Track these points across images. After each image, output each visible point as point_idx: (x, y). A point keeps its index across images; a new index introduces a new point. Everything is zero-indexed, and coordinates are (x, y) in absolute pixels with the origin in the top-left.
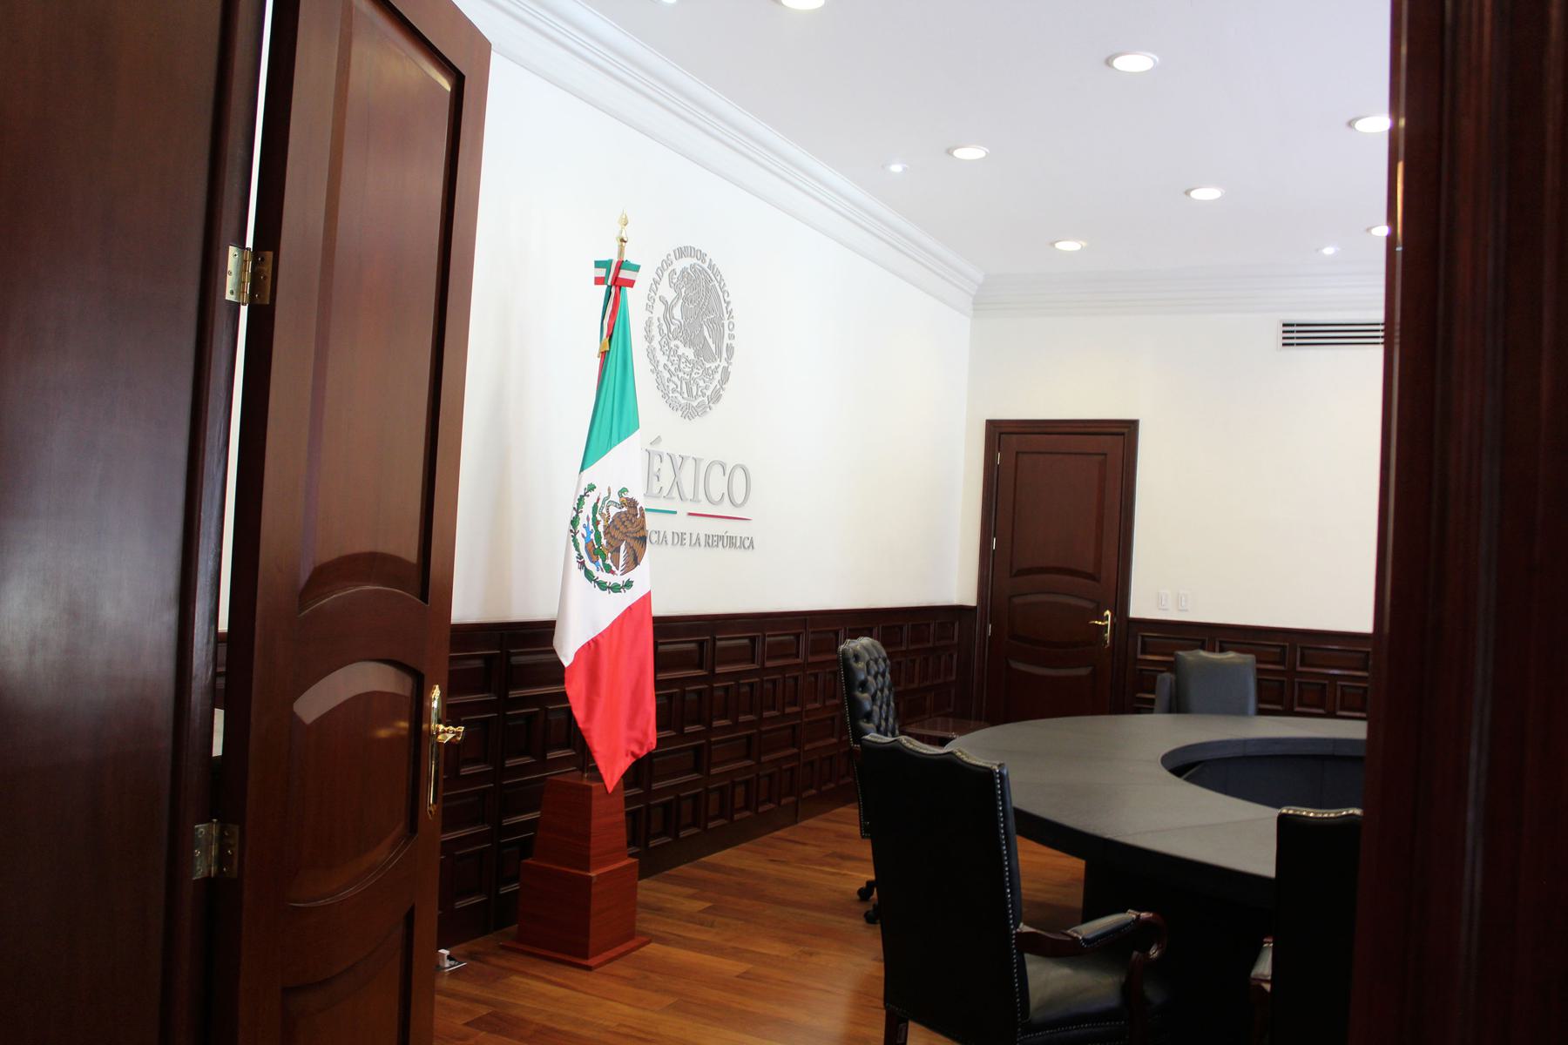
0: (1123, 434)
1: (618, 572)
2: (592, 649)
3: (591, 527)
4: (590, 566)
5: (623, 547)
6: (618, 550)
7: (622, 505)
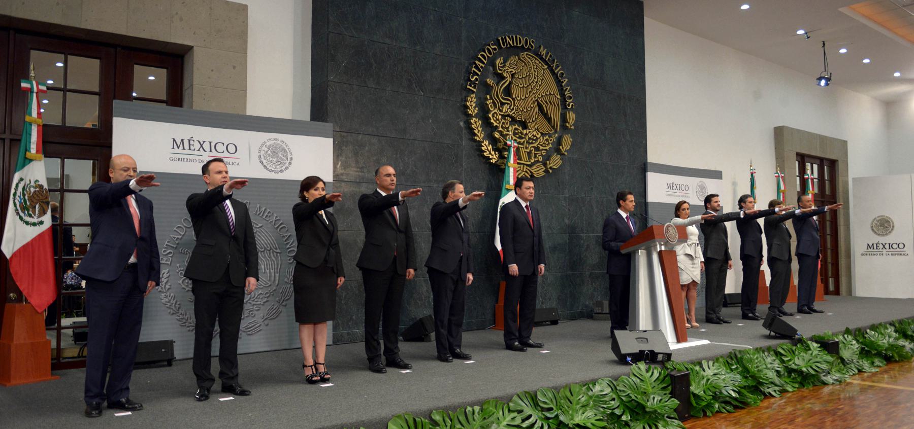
0: (722, 179)
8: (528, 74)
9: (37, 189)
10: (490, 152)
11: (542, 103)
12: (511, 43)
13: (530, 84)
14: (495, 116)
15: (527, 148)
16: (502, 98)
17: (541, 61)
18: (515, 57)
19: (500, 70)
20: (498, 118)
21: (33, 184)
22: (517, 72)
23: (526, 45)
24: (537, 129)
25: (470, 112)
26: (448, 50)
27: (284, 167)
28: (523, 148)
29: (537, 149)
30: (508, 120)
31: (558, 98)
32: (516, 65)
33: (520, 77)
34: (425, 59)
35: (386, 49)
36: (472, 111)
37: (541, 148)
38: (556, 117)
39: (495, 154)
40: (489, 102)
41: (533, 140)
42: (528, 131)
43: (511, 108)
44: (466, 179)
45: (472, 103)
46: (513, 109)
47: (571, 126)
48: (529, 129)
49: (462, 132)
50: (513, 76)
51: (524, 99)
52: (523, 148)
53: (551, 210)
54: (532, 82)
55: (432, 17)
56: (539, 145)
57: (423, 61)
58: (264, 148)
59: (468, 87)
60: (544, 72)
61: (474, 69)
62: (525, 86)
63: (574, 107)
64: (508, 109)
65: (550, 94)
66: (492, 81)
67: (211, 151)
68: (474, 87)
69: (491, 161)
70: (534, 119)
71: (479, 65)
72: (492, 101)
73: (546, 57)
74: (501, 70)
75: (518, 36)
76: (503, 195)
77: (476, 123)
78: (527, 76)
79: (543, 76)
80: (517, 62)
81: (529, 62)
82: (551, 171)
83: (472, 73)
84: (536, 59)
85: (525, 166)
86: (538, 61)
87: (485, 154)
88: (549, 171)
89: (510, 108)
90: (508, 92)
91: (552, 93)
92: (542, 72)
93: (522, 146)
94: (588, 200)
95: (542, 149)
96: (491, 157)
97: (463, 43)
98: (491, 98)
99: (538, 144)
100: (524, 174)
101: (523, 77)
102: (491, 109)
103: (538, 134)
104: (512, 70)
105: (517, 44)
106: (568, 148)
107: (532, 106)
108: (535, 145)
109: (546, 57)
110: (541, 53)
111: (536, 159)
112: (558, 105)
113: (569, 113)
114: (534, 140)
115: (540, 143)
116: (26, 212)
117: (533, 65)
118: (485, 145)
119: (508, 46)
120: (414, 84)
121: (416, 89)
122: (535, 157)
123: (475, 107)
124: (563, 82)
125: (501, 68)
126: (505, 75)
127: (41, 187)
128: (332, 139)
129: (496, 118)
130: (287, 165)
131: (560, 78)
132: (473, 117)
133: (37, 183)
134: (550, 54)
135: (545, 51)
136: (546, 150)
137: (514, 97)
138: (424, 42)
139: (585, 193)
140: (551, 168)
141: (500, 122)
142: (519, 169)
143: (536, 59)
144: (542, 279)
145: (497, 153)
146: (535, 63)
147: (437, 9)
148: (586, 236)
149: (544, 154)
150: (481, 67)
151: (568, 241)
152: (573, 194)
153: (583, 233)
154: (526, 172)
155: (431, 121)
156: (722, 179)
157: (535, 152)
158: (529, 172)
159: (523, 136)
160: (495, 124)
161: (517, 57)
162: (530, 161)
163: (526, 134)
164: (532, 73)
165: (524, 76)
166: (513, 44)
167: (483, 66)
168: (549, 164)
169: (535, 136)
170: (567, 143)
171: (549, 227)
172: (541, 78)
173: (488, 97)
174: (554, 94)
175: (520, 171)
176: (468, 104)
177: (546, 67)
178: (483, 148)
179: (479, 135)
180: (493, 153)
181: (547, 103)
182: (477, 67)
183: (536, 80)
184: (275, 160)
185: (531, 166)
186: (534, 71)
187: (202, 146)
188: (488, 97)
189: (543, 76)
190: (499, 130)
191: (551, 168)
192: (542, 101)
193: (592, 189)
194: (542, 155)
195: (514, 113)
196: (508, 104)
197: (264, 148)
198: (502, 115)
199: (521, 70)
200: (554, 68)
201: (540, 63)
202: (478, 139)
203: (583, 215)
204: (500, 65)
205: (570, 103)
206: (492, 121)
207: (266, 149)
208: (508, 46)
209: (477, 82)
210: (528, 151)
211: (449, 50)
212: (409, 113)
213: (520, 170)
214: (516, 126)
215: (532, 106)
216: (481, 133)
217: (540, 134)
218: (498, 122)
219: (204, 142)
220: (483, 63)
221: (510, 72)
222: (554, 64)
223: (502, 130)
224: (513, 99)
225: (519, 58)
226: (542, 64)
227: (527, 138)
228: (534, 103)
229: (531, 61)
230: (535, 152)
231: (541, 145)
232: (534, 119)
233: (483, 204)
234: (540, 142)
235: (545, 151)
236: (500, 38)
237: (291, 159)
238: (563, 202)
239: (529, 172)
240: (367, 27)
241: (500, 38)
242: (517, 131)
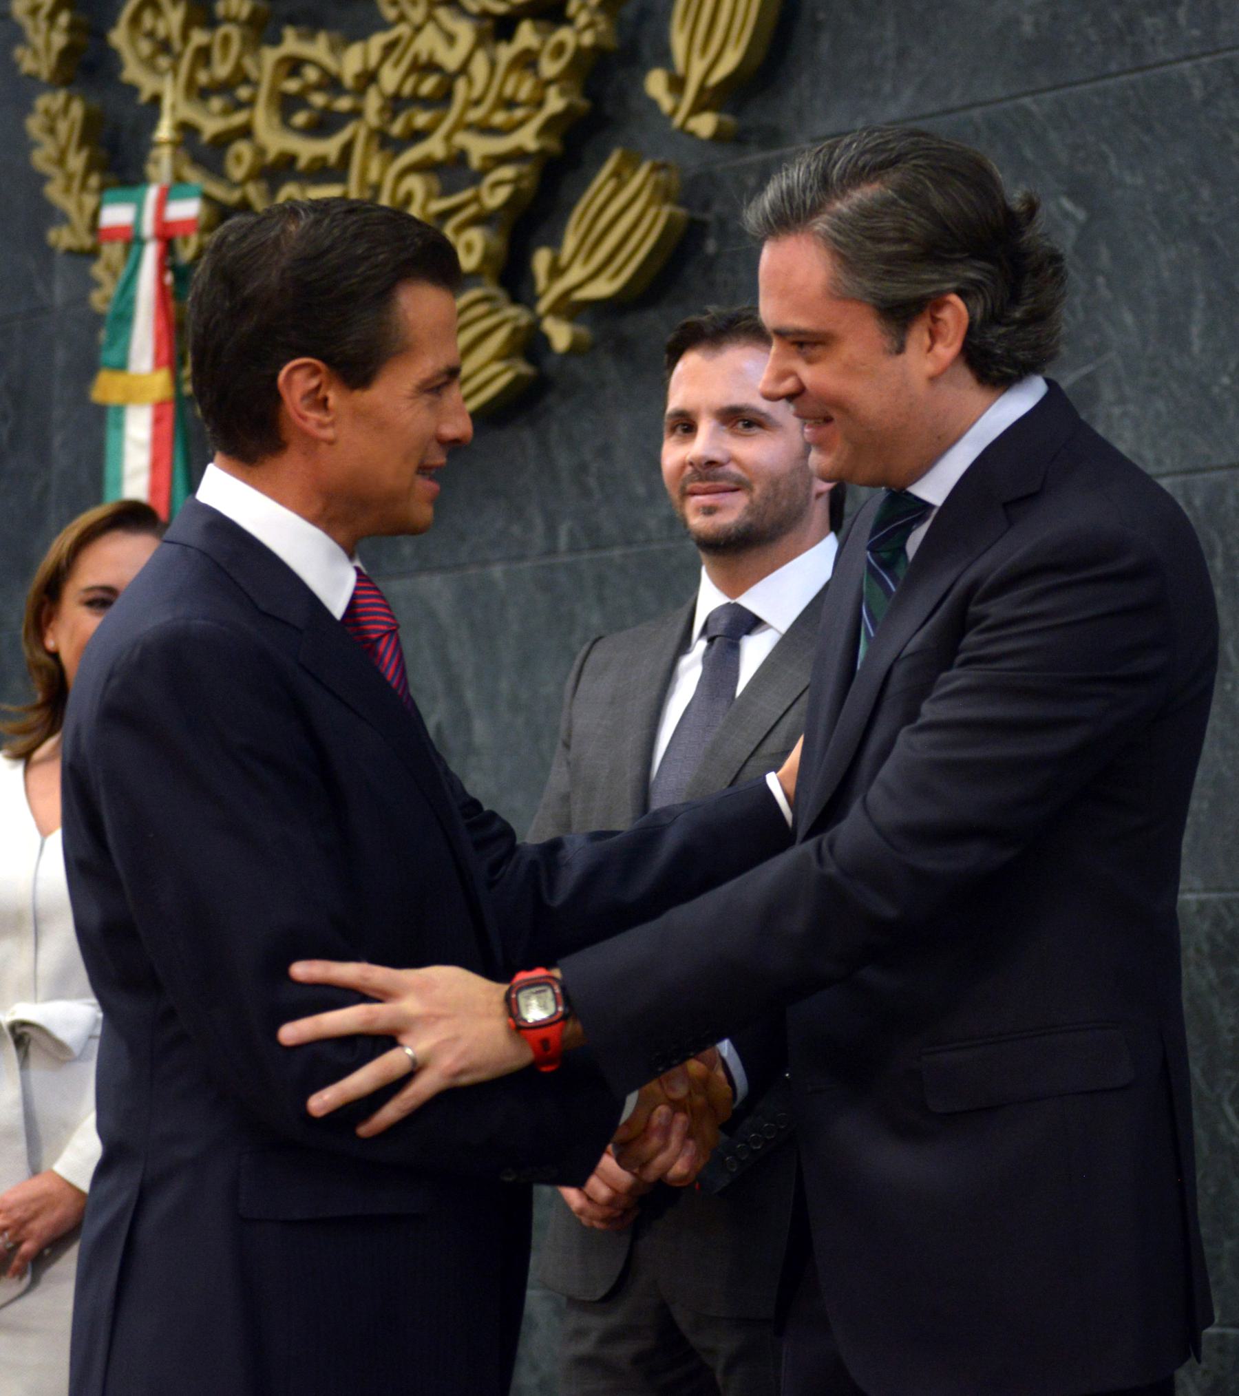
41: (417, 101)
108: (435, 147)
114: (426, 103)
123: (52, 17)
159: (344, 104)
163: (369, 78)
168: (556, 271)
169: (427, 67)
191: (568, 308)
216: (84, 186)
217: (465, 32)
227: (373, 102)
235: (507, 172)
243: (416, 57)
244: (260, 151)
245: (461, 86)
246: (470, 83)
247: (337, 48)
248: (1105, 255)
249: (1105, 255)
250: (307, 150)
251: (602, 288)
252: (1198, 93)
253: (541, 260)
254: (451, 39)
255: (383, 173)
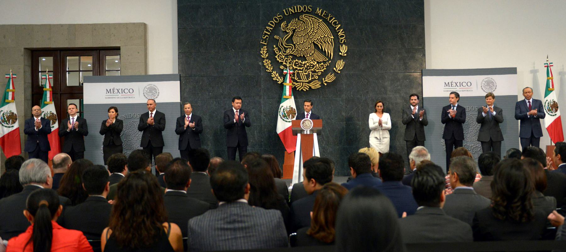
0: (516, 74)
1: (290, 119)
2: (284, 132)
3: (283, 112)
4: (283, 118)
5: (290, 115)
6: (289, 116)
7: (290, 108)
8: (306, 27)
9: (51, 115)
10: (277, 77)
11: (318, 44)
12: (293, 11)
13: (307, 33)
14: (280, 56)
15: (305, 72)
16: (286, 45)
17: (317, 18)
18: (296, 19)
19: (283, 29)
20: (282, 57)
21: (49, 113)
22: (296, 28)
23: (305, 10)
24: (314, 59)
25: (263, 57)
26: (250, 24)
27: (156, 97)
28: (303, 73)
29: (314, 72)
30: (290, 57)
31: (331, 39)
32: (296, 24)
33: (299, 31)
34: (235, 32)
35: (211, 31)
36: (264, 56)
37: (317, 71)
38: (330, 50)
39: (281, 78)
40: (276, 49)
42: (306, 62)
43: (293, 50)
44: (264, 94)
45: (264, 52)
46: (294, 50)
47: (344, 54)
48: (308, 61)
49: (260, 68)
50: (294, 31)
51: (302, 44)
52: (303, 73)
53: (330, 108)
54: (310, 32)
55: (239, 7)
56: (315, 70)
57: (234, 33)
58: (146, 89)
59: (261, 42)
60: (319, 24)
61: (265, 32)
62: (303, 35)
63: (345, 42)
64: (290, 51)
65: (324, 36)
66: (278, 37)
67: (122, 93)
68: (265, 42)
69: (278, 83)
70: (311, 54)
71: (269, 29)
72: (277, 48)
73: (321, 14)
74: (285, 29)
75: (298, 6)
76: (282, 102)
77: (267, 63)
78: (304, 29)
79: (319, 26)
80: (297, 22)
81: (306, 20)
82: (326, 84)
83: (263, 34)
84: (312, 17)
85: (304, 83)
86: (314, 18)
87: (274, 79)
88: (324, 84)
89: (291, 50)
90: (290, 40)
91: (326, 36)
92: (318, 25)
93: (302, 72)
94: (364, 100)
95: (318, 72)
96: (278, 80)
97: (261, 18)
98: (276, 47)
99: (315, 68)
100: (304, 88)
101: (301, 30)
102: (277, 53)
103: (314, 63)
104: (294, 27)
105: (297, 10)
106: (341, 68)
107: (309, 46)
109: (321, 14)
110: (317, 12)
111: (312, 78)
112: (332, 43)
113: (342, 46)
115: (317, 68)
116: (286, 118)
117: (310, 21)
118: (274, 74)
119: (291, 13)
120: (228, 47)
121: (230, 49)
122: (312, 76)
123: (266, 54)
124: (336, 27)
125: (284, 28)
126: (288, 31)
127: (53, 114)
128: (179, 82)
129: (281, 57)
130: (157, 96)
131: (334, 25)
132: (265, 59)
133: (51, 112)
134: (325, 11)
135: (320, 11)
136: (321, 72)
137: (295, 43)
138: (235, 22)
139: (361, 95)
140: (326, 82)
141: (283, 60)
142: (300, 85)
143: (312, 17)
144: (323, 150)
145: (282, 77)
146: (312, 19)
147: (242, 2)
148: (361, 123)
149: (320, 74)
150: (271, 30)
151: (345, 126)
152: (349, 96)
153: (359, 121)
154: (305, 86)
155: (239, 64)
156: (516, 74)
157: (313, 74)
158: (307, 86)
159: (303, 65)
160: (280, 61)
161: (297, 19)
162: (308, 80)
163: (305, 64)
164: (309, 27)
165: (302, 29)
166: (294, 11)
167: (272, 29)
169: (312, 64)
170: (340, 65)
171: (329, 118)
172: (317, 28)
173: (275, 46)
174: (328, 36)
175: (300, 87)
176: (261, 52)
177: (321, 20)
178: (272, 76)
179: (269, 69)
180: (279, 78)
181: (322, 43)
182: (267, 30)
183: (312, 30)
184: (151, 94)
185: (309, 82)
186: (311, 25)
187: (118, 91)
188: (275, 46)
189: (319, 26)
190: (283, 64)
191: (326, 82)
192: (317, 42)
193: (367, 92)
194: (318, 75)
195: (295, 53)
196: (290, 48)
197: (146, 89)
198: (285, 55)
199: (300, 26)
200: (328, 20)
201: (316, 19)
202: (268, 71)
203: (359, 109)
204: (284, 26)
205: (342, 39)
206: (278, 59)
207: (147, 90)
208: (291, 13)
209: (267, 39)
210: (307, 74)
211: (251, 23)
212: (225, 62)
213: (300, 85)
214: (297, 60)
215: (309, 46)
216: (271, 67)
218: (282, 60)
219: (119, 89)
220: (272, 27)
221: (292, 29)
222: (328, 17)
223: (285, 64)
224: (295, 45)
225: (299, 19)
226: (317, 19)
227: (306, 66)
228: (311, 44)
229: (308, 19)
230: (313, 74)
231: (318, 69)
232: (311, 54)
233: (276, 107)
234: (316, 67)
235: (321, 73)
236: (284, 10)
237: (159, 93)
238: (340, 102)
239: (307, 86)
240: (199, 22)
241: (284, 10)
242: (297, 63)
243: (311, 63)
244: (293, 68)
245: (315, 66)
246: (316, 66)
247: (302, 62)
248: (369, 84)
249: (369, 84)
250: (298, 68)
251: (329, 81)
252: (376, 75)
253: (323, 79)
254: (314, 63)
255: (307, 71)
